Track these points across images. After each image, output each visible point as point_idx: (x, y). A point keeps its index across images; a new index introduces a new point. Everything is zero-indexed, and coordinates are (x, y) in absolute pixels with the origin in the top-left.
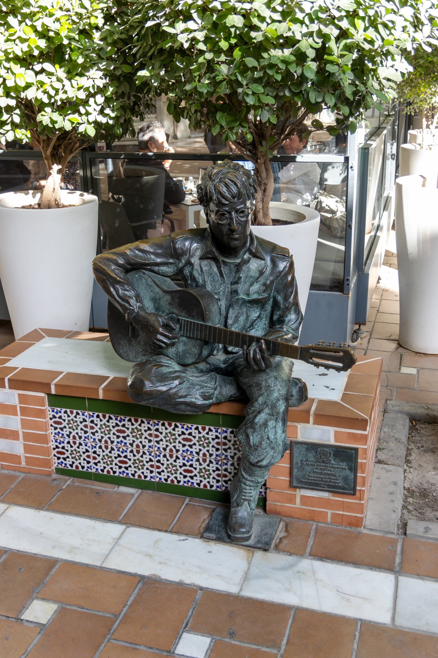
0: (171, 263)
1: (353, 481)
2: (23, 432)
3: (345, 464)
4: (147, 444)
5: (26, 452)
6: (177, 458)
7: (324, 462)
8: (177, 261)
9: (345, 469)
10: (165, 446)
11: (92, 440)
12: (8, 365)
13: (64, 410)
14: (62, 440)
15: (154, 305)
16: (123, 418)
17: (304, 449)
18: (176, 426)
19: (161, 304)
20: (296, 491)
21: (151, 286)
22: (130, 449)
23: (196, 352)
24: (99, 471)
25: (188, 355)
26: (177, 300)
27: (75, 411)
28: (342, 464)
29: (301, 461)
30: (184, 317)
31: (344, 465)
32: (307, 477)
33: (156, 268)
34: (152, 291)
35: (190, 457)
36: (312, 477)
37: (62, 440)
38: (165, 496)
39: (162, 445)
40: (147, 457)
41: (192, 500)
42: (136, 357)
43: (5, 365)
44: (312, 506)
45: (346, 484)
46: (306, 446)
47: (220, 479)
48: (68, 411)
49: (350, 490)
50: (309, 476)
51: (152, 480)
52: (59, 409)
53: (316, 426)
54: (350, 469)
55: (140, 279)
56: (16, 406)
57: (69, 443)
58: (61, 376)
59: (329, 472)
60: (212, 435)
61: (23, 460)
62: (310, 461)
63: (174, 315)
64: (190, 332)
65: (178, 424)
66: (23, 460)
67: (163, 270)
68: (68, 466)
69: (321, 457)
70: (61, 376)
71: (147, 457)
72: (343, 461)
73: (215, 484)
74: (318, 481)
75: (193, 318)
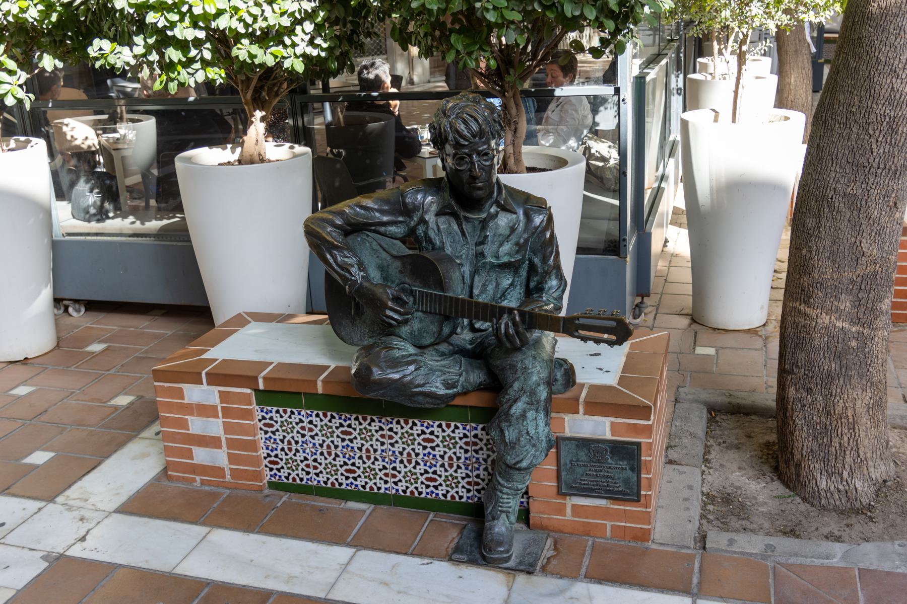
0: (401, 222)
2: (227, 438)
3: (625, 463)
4: (380, 448)
5: (231, 463)
6: (417, 463)
7: (599, 461)
9: (625, 469)
11: (311, 445)
12: (206, 356)
13: (275, 409)
14: (274, 446)
17: (574, 447)
21: (377, 251)
22: (358, 455)
23: (435, 329)
24: (322, 483)
25: (425, 335)
27: (289, 410)
29: (571, 461)
30: (418, 287)
31: (624, 464)
33: (382, 229)
35: (434, 462)
37: (274, 446)
38: (404, 512)
39: (398, 448)
40: (379, 464)
43: (202, 357)
44: (587, 518)
47: (471, 488)
48: (281, 409)
52: (269, 408)
53: (587, 417)
54: (632, 469)
56: (216, 406)
57: (283, 449)
58: (271, 367)
61: (227, 472)
65: (416, 421)
66: (227, 472)
68: (283, 478)
70: (271, 367)
71: (379, 464)
72: (622, 459)
73: (465, 495)
75: (429, 287)
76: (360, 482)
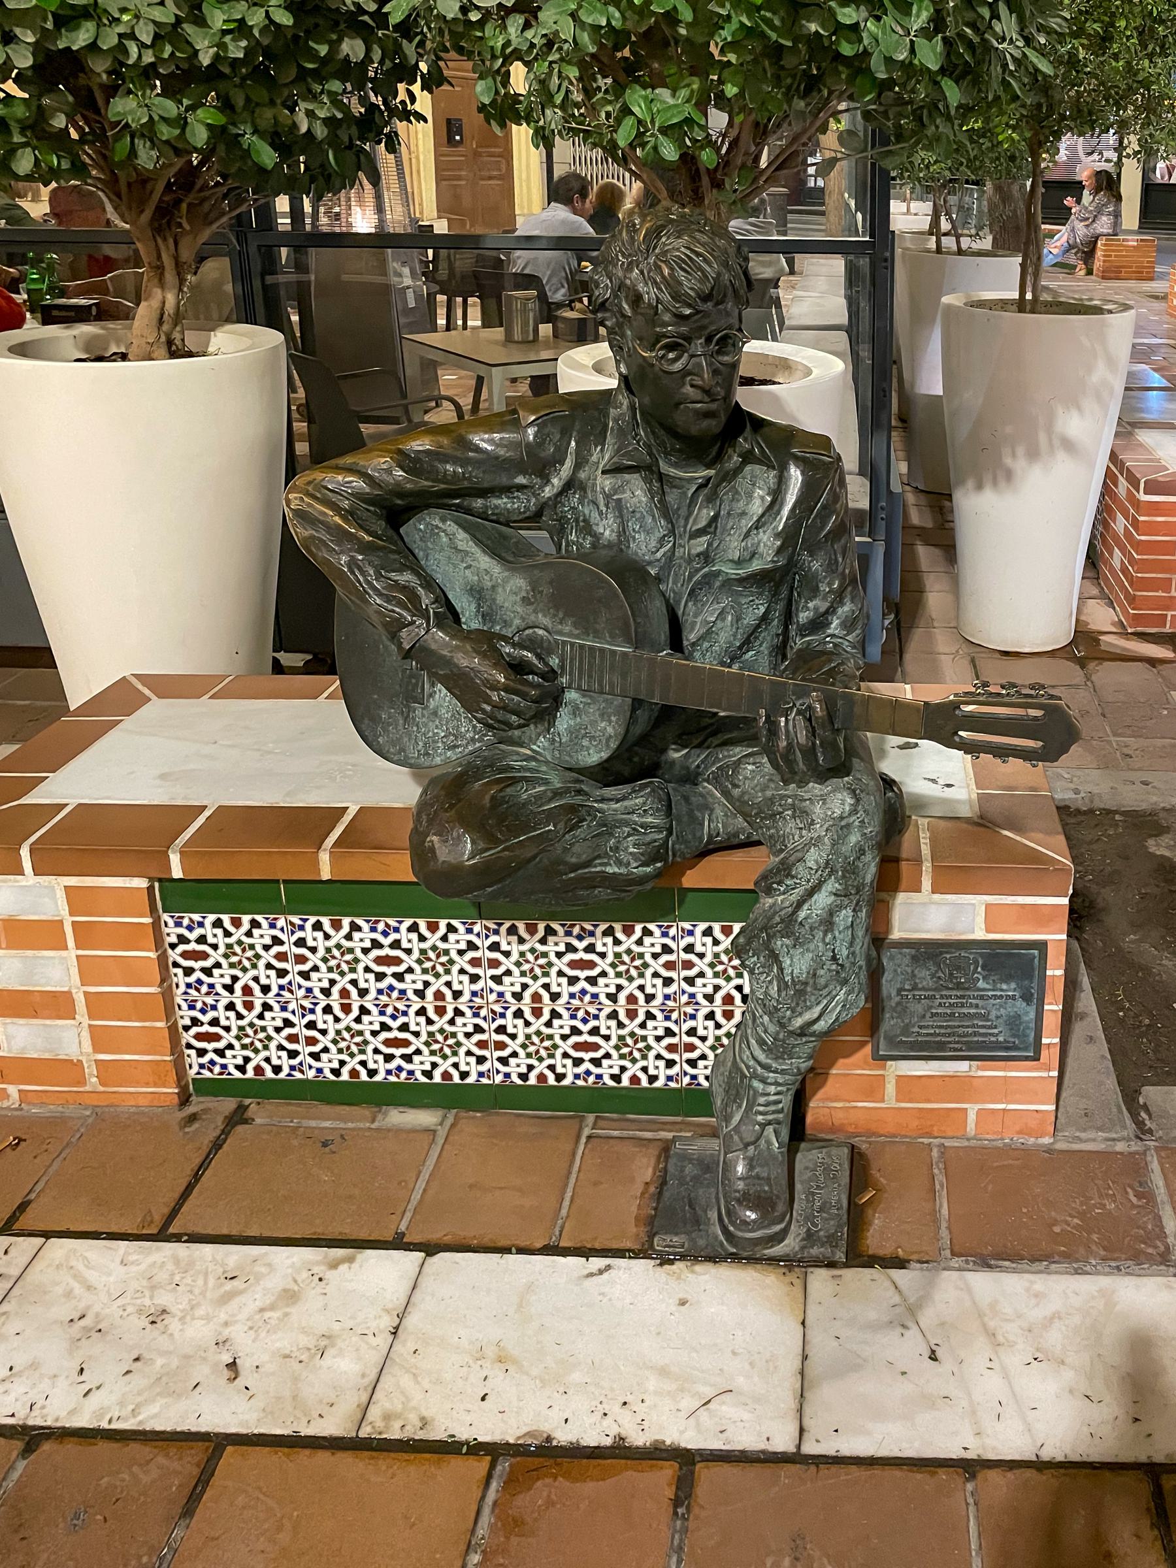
0: (521, 488)
1: (1032, 1025)
2: (85, 993)
3: (1013, 985)
4: (467, 988)
5: (96, 1049)
6: (555, 1014)
7: (959, 986)
8: (537, 481)
9: (1013, 998)
10: (518, 988)
11: (302, 992)
12: (33, 798)
13: (212, 918)
14: (210, 1000)
15: (479, 606)
16: (588, 927)
17: (907, 960)
18: (647, 932)
19: (500, 599)
20: (884, 1067)
21: (467, 553)
22: (416, 1007)
23: (610, 730)
24: (327, 1073)
25: (585, 743)
26: (547, 590)
27: (246, 919)
28: (1004, 987)
29: (899, 991)
30: (570, 635)
31: (1009, 988)
32: (916, 1029)
33: (479, 503)
34: (469, 567)
35: (592, 1011)
36: (927, 1027)
37: (210, 1000)
38: (523, 1121)
39: (510, 986)
40: (467, 1022)
41: (601, 1123)
42: (427, 754)
43: (26, 800)
44: (928, 1101)
45: (1014, 1036)
46: (913, 951)
47: (676, 1057)
48: (226, 919)
49: (1026, 1049)
50: (920, 1027)
51: (673, 1085)
52: (196, 917)
53: (937, 897)
54: (1027, 998)
55: (433, 534)
56: (61, 922)
57: (230, 1007)
58: (201, 820)
59: (972, 1011)
60: (556, 944)
61: (90, 1070)
62: (923, 989)
63: (540, 632)
64: (590, 676)
65: (652, 926)
66: (90, 1070)
67: (496, 507)
68: (231, 1069)
69: (951, 974)
70: (201, 820)
71: (467, 1022)
72: (1007, 979)
73: (663, 1073)
74: (943, 1035)
75: (597, 635)
76: (419, 1065)
